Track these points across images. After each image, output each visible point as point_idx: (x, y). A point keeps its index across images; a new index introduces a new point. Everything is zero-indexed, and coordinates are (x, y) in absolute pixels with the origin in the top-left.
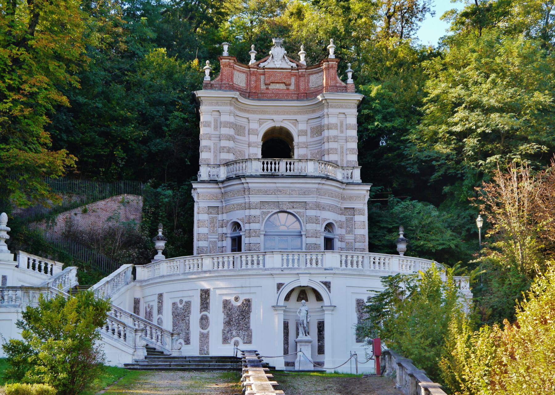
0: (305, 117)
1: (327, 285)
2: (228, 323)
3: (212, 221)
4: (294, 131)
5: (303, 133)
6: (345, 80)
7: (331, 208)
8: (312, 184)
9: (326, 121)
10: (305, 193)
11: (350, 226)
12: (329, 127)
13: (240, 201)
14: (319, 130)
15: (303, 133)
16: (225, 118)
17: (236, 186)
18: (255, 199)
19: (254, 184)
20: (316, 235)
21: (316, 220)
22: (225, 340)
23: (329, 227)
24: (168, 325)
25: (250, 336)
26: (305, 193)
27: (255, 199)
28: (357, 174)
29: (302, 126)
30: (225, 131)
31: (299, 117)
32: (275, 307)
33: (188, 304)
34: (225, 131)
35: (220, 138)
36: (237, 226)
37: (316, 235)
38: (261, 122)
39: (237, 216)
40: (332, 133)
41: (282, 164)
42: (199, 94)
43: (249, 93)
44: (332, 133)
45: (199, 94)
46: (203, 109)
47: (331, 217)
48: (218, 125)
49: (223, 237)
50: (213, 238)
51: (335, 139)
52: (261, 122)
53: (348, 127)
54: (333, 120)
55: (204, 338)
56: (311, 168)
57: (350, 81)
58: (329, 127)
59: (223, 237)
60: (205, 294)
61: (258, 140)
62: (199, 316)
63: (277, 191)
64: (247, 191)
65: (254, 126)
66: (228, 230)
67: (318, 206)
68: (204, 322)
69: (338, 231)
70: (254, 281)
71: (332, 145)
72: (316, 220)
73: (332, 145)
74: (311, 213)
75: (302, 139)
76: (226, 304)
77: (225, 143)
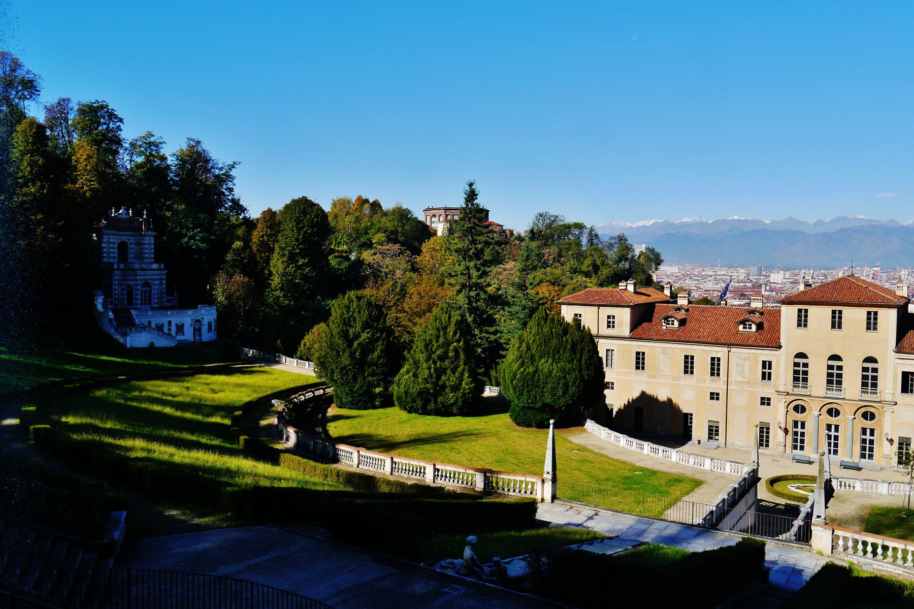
0: (133, 238)
1: (203, 318)
5: (131, 244)
8: (156, 272)
10: (153, 275)
12: (146, 244)
13: (132, 278)
16: (111, 240)
17: (131, 272)
18: (138, 278)
19: (139, 272)
25: (184, 333)
26: (153, 275)
27: (138, 278)
29: (132, 241)
31: (131, 238)
32: (191, 325)
33: (163, 325)
35: (110, 248)
36: (130, 286)
38: (117, 239)
40: (147, 246)
46: (104, 236)
48: (109, 243)
50: (119, 290)
51: (147, 249)
53: (151, 244)
54: (147, 242)
57: (152, 226)
58: (146, 244)
59: (123, 290)
60: (170, 323)
62: (168, 328)
64: (137, 275)
65: (115, 241)
70: (185, 318)
71: (147, 251)
74: (155, 282)
75: (132, 246)
76: (176, 325)
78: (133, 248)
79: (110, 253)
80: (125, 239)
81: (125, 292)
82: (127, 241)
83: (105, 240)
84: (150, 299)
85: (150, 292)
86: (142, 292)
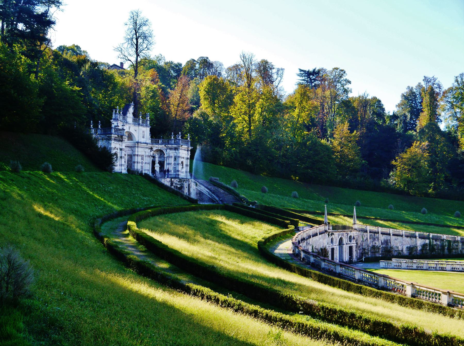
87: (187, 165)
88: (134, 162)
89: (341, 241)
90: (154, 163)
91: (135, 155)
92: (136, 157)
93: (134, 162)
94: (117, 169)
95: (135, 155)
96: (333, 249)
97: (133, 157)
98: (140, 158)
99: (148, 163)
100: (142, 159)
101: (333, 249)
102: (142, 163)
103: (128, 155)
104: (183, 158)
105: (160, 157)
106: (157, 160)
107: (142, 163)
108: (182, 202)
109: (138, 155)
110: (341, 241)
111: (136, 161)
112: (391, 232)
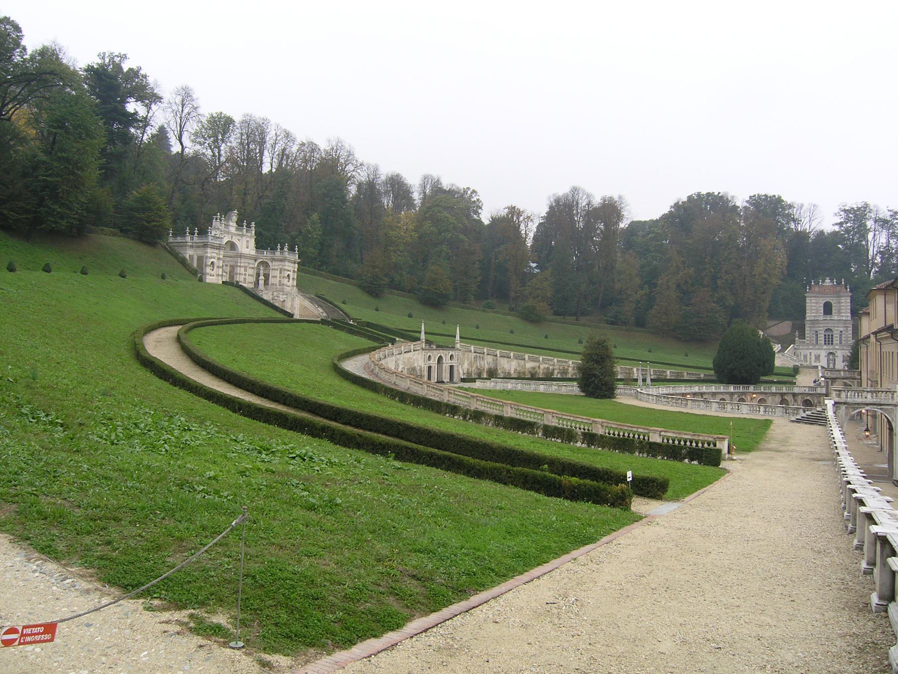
2: (815, 359)
3: (810, 330)
4: (832, 303)
5: (835, 303)
6: (847, 289)
7: (841, 327)
9: (841, 301)
11: (847, 331)
12: (842, 303)
14: (839, 303)
15: (835, 303)
16: (813, 301)
19: (821, 322)
20: (837, 334)
21: (837, 330)
22: (815, 362)
23: (841, 331)
24: (802, 359)
27: (821, 325)
28: (849, 318)
29: (835, 301)
30: (813, 304)
34: (813, 304)
36: (816, 331)
37: (837, 334)
39: (817, 329)
40: (843, 304)
41: (828, 317)
42: (806, 295)
43: (819, 293)
44: (843, 304)
45: (806, 295)
47: (841, 329)
49: (813, 334)
51: (844, 306)
52: (823, 300)
54: (843, 301)
55: (811, 361)
56: (836, 318)
58: (842, 303)
61: (822, 305)
63: (827, 323)
64: (819, 323)
66: (814, 332)
67: (838, 327)
68: (810, 358)
69: (843, 332)
71: (843, 308)
72: (837, 330)
73: (843, 308)
76: (815, 355)
77: (813, 308)
78: (836, 306)
79: (812, 310)
80: (828, 300)
81: (814, 336)
82: (831, 301)
83: (807, 301)
84: (832, 341)
85: (832, 335)
86: (825, 335)
87: (293, 279)
88: (237, 274)
89: (440, 359)
90: (258, 275)
91: (237, 266)
92: (239, 268)
93: (237, 274)
94: (209, 279)
95: (237, 266)
96: (430, 368)
97: (236, 268)
98: (243, 269)
99: (252, 276)
100: (245, 270)
101: (430, 368)
102: (245, 275)
103: (230, 266)
104: (214, 258)
105: (264, 270)
106: (262, 272)
107: (245, 275)
108: (280, 316)
109: (240, 266)
110: (440, 359)
111: (238, 272)
112: (485, 351)
